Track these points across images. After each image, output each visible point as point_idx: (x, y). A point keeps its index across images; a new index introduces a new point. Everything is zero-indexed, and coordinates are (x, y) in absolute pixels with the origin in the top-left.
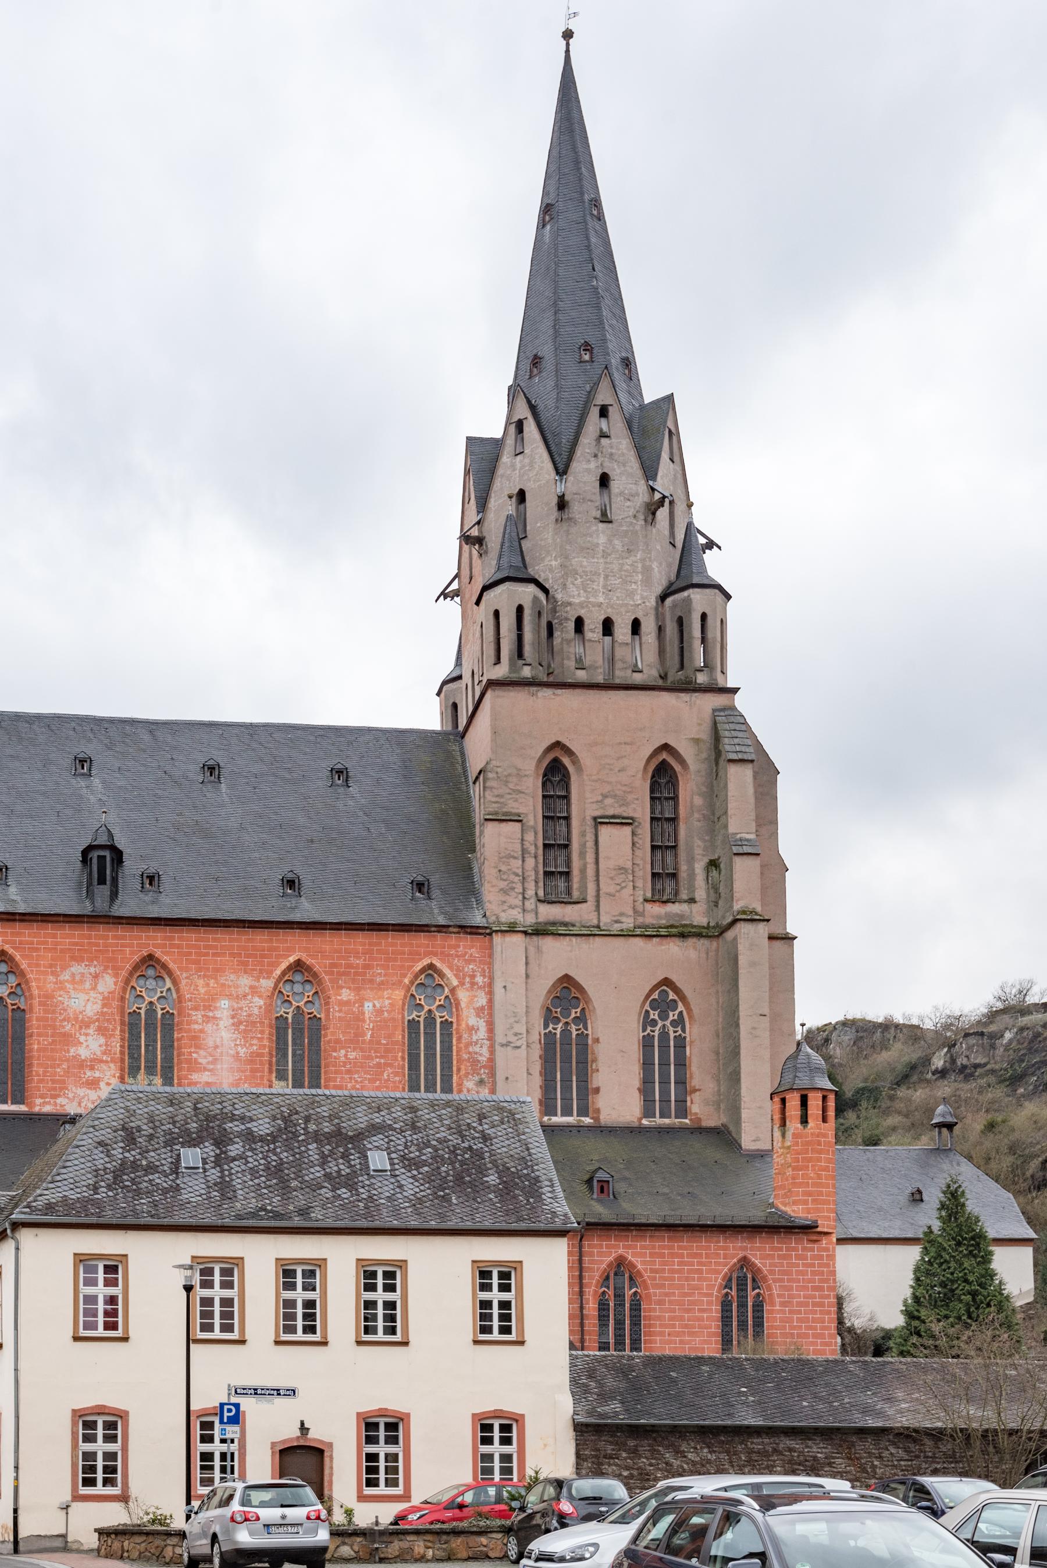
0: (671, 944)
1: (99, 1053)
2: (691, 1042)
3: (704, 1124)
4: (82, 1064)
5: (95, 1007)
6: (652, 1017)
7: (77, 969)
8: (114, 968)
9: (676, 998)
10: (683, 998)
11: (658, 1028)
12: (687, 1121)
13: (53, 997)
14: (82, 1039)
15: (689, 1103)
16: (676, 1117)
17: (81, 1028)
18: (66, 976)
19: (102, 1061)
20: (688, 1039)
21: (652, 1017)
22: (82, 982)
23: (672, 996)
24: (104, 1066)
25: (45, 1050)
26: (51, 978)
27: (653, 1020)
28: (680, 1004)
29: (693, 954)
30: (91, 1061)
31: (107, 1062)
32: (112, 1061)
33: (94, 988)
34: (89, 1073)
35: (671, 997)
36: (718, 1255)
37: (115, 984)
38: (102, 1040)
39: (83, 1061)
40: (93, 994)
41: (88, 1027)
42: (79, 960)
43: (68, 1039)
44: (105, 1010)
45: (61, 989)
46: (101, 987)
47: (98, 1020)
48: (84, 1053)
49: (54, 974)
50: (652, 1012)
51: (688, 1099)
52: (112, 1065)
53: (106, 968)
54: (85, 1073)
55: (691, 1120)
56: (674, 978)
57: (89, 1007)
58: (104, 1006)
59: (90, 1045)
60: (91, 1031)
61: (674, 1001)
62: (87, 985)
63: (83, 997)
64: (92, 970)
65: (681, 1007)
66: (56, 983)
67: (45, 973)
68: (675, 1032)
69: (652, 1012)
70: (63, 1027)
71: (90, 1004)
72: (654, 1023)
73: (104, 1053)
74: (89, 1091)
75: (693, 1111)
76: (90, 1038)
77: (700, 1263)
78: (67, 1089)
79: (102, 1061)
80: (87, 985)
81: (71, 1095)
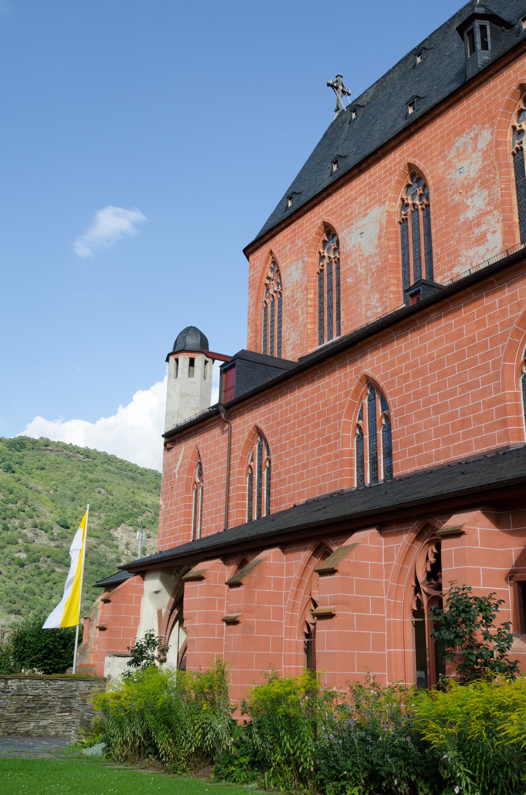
1: (483, 207)
4: (470, 226)
5: (476, 166)
7: (460, 142)
8: (490, 120)
13: (444, 178)
14: (469, 202)
17: (467, 192)
18: (453, 153)
19: (487, 213)
22: (464, 150)
24: (488, 217)
25: (441, 229)
26: (442, 163)
30: (477, 219)
31: (491, 211)
32: (495, 209)
33: (475, 150)
34: (476, 231)
37: (492, 134)
38: (485, 193)
39: (471, 221)
40: (474, 156)
41: (472, 188)
42: (458, 134)
43: (457, 209)
44: (486, 163)
45: (448, 169)
46: (480, 147)
47: (480, 177)
48: (471, 214)
49: (444, 158)
52: (496, 212)
53: (483, 124)
54: (473, 233)
57: (472, 170)
58: (484, 160)
59: (477, 202)
60: (475, 191)
62: (470, 150)
63: (465, 164)
64: (472, 134)
66: (445, 165)
67: (437, 162)
70: (453, 200)
71: (472, 166)
73: (487, 205)
74: (478, 248)
76: (475, 198)
78: (460, 256)
79: (487, 213)
80: (470, 150)
81: (463, 260)
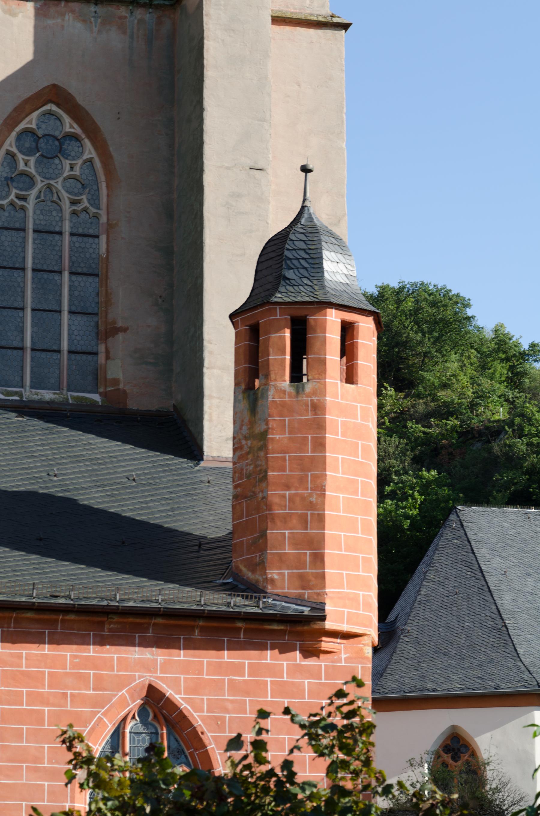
0: (69, 17)
2: (110, 227)
3: (133, 405)
6: (22, 166)
9: (77, 130)
10: (93, 132)
11: (34, 193)
12: (96, 397)
15: (102, 358)
16: (69, 390)
20: (104, 219)
21: (22, 166)
23: (69, 125)
27: (24, 174)
28: (87, 143)
29: (115, 39)
35: (68, 129)
36: (83, 679)
50: (20, 157)
51: (102, 348)
55: (104, 395)
56: (74, 87)
61: (74, 137)
65: (89, 151)
68: (73, 203)
69: (20, 157)
72: (28, 180)
75: (110, 376)
77: (33, 698)
